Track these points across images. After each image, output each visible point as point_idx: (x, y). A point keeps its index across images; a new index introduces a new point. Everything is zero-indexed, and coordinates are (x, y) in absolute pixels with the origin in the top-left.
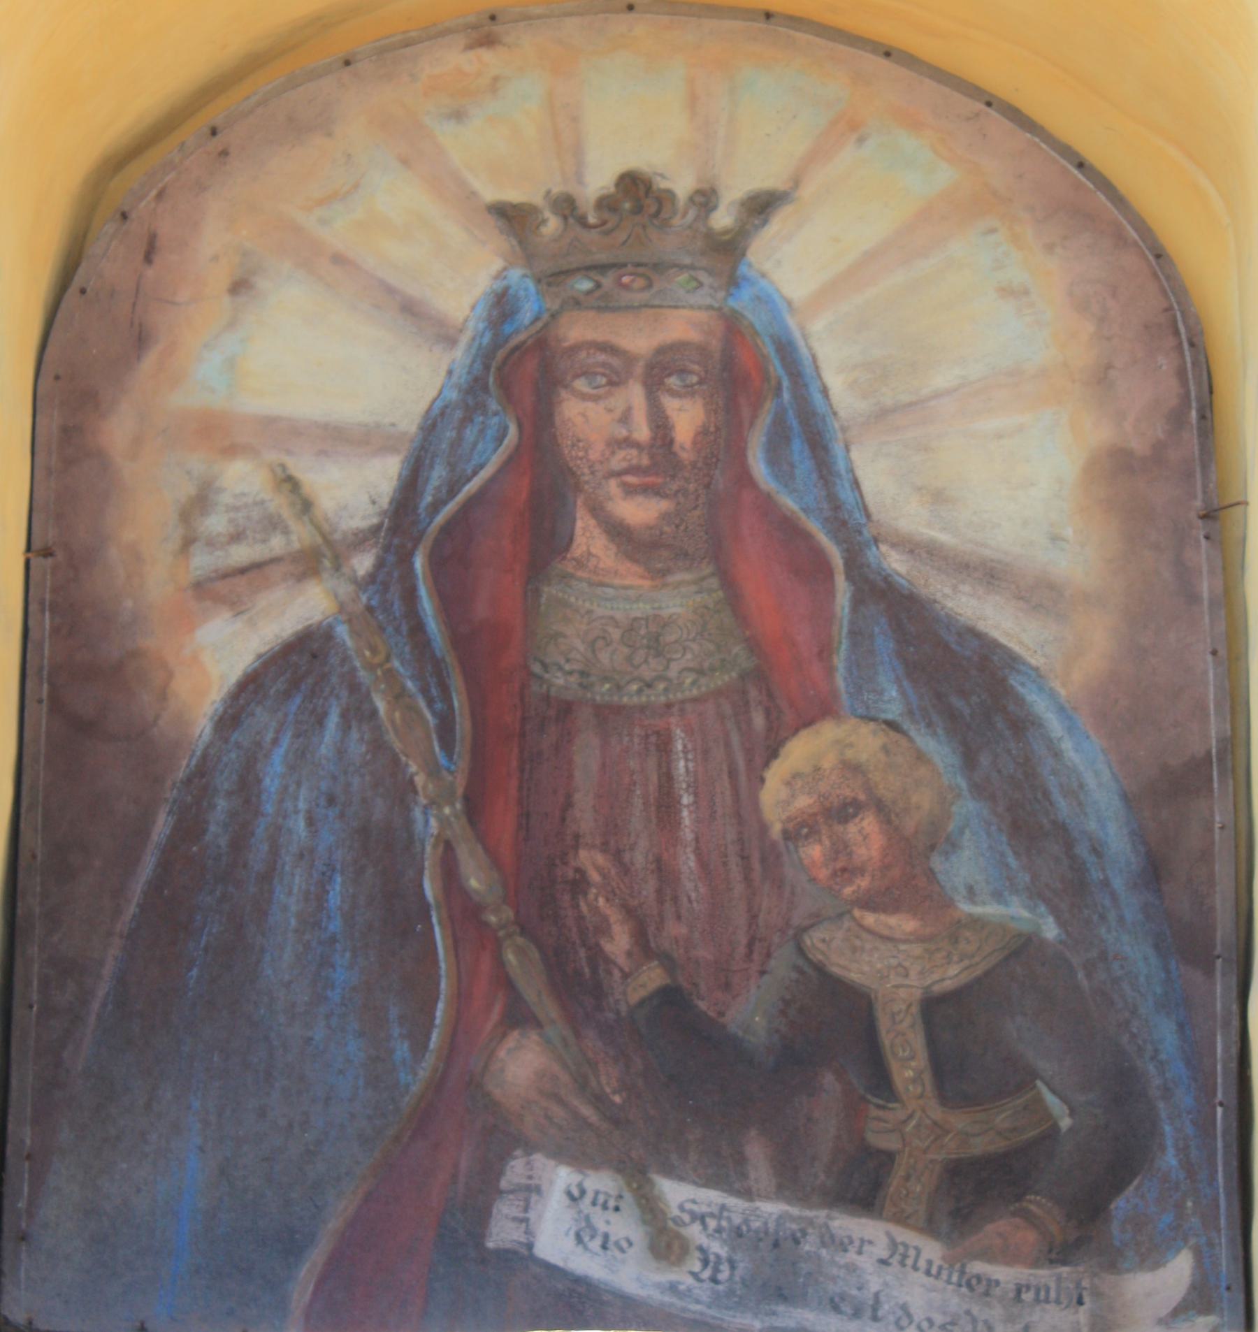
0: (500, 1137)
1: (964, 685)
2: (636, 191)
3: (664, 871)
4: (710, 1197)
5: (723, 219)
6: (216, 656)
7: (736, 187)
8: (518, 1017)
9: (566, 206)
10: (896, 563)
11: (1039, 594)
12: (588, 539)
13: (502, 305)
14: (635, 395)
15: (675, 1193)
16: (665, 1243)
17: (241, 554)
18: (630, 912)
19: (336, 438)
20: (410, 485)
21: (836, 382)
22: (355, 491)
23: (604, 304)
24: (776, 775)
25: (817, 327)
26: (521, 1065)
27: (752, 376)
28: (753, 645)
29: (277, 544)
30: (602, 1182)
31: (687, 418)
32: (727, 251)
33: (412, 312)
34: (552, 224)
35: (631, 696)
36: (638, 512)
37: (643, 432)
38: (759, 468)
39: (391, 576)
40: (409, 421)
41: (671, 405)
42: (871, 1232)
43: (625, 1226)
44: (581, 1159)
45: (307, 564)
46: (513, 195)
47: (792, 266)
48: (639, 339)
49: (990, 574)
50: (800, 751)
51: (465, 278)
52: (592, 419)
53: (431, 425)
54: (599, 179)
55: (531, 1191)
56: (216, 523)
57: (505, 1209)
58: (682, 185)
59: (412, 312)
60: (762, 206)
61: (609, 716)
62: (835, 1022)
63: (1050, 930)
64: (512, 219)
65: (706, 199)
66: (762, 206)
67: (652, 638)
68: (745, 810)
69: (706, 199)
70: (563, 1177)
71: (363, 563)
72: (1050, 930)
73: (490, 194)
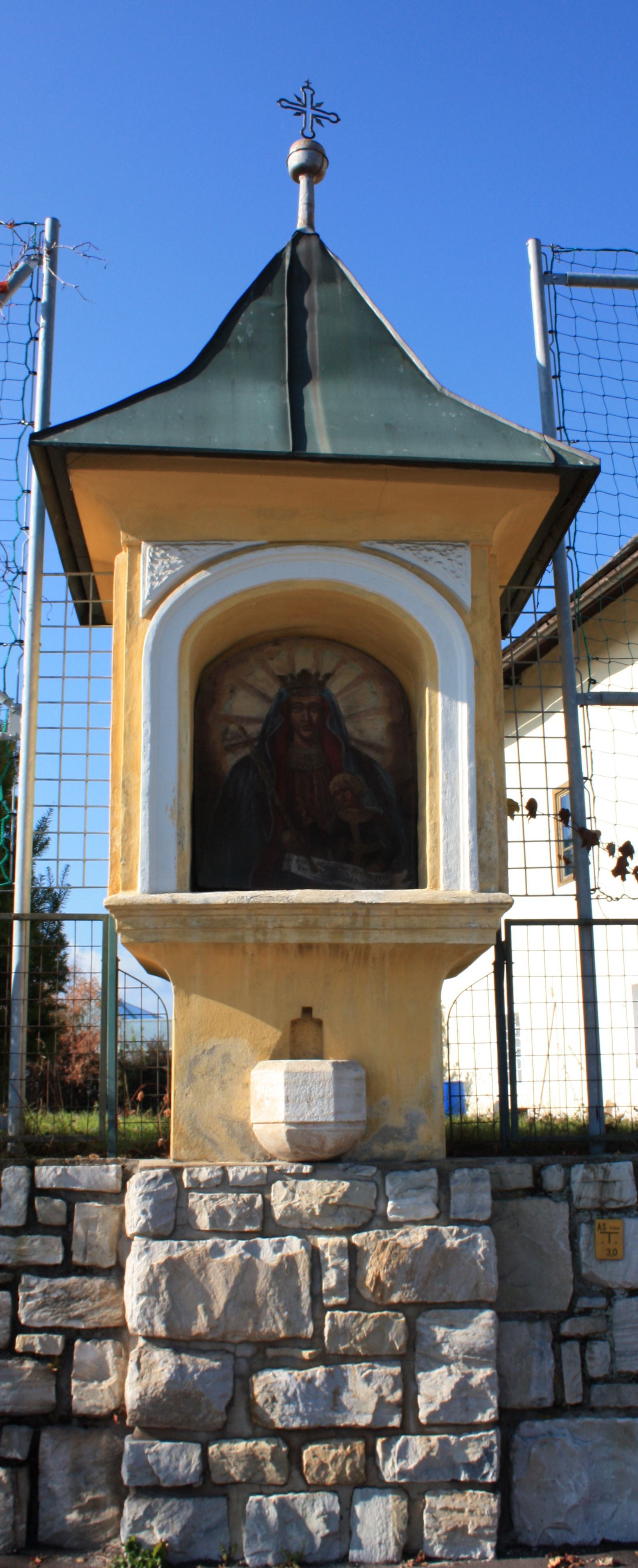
1: (365, 766)
2: (305, 673)
4: (321, 860)
5: (321, 679)
6: (231, 760)
7: (323, 672)
9: (292, 676)
10: (353, 744)
11: (378, 749)
12: (297, 739)
13: (280, 695)
14: (305, 712)
16: (314, 869)
17: (233, 742)
19: (251, 720)
21: (342, 710)
22: (254, 730)
25: (339, 699)
26: (287, 837)
27: (327, 708)
29: (240, 740)
30: (302, 858)
31: (315, 717)
32: (322, 686)
33: (263, 696)
34: (289, 680)
36: (306, 734)
37: (307, 719)
38: (328, 725)
40: (264, 716)
41: (312, 714)
42: (350, 867)
45: (246, 744)
46: (282, 674)
47: (334, 687)
48: (306, 701)
49: (370, 745)
50: (336, 779)
51: (273, 690)
52: (297, 716)
54: (298, 670)
56: (229, 736)
58: (313, 672)
60: (328, 676)
63: (382, 812)
64: (282, 679)
65: (318, 674)
66: (328, 676)
69: (318, 674)
71: (256, 744)
72: (382, 812)
73: (278, 673)
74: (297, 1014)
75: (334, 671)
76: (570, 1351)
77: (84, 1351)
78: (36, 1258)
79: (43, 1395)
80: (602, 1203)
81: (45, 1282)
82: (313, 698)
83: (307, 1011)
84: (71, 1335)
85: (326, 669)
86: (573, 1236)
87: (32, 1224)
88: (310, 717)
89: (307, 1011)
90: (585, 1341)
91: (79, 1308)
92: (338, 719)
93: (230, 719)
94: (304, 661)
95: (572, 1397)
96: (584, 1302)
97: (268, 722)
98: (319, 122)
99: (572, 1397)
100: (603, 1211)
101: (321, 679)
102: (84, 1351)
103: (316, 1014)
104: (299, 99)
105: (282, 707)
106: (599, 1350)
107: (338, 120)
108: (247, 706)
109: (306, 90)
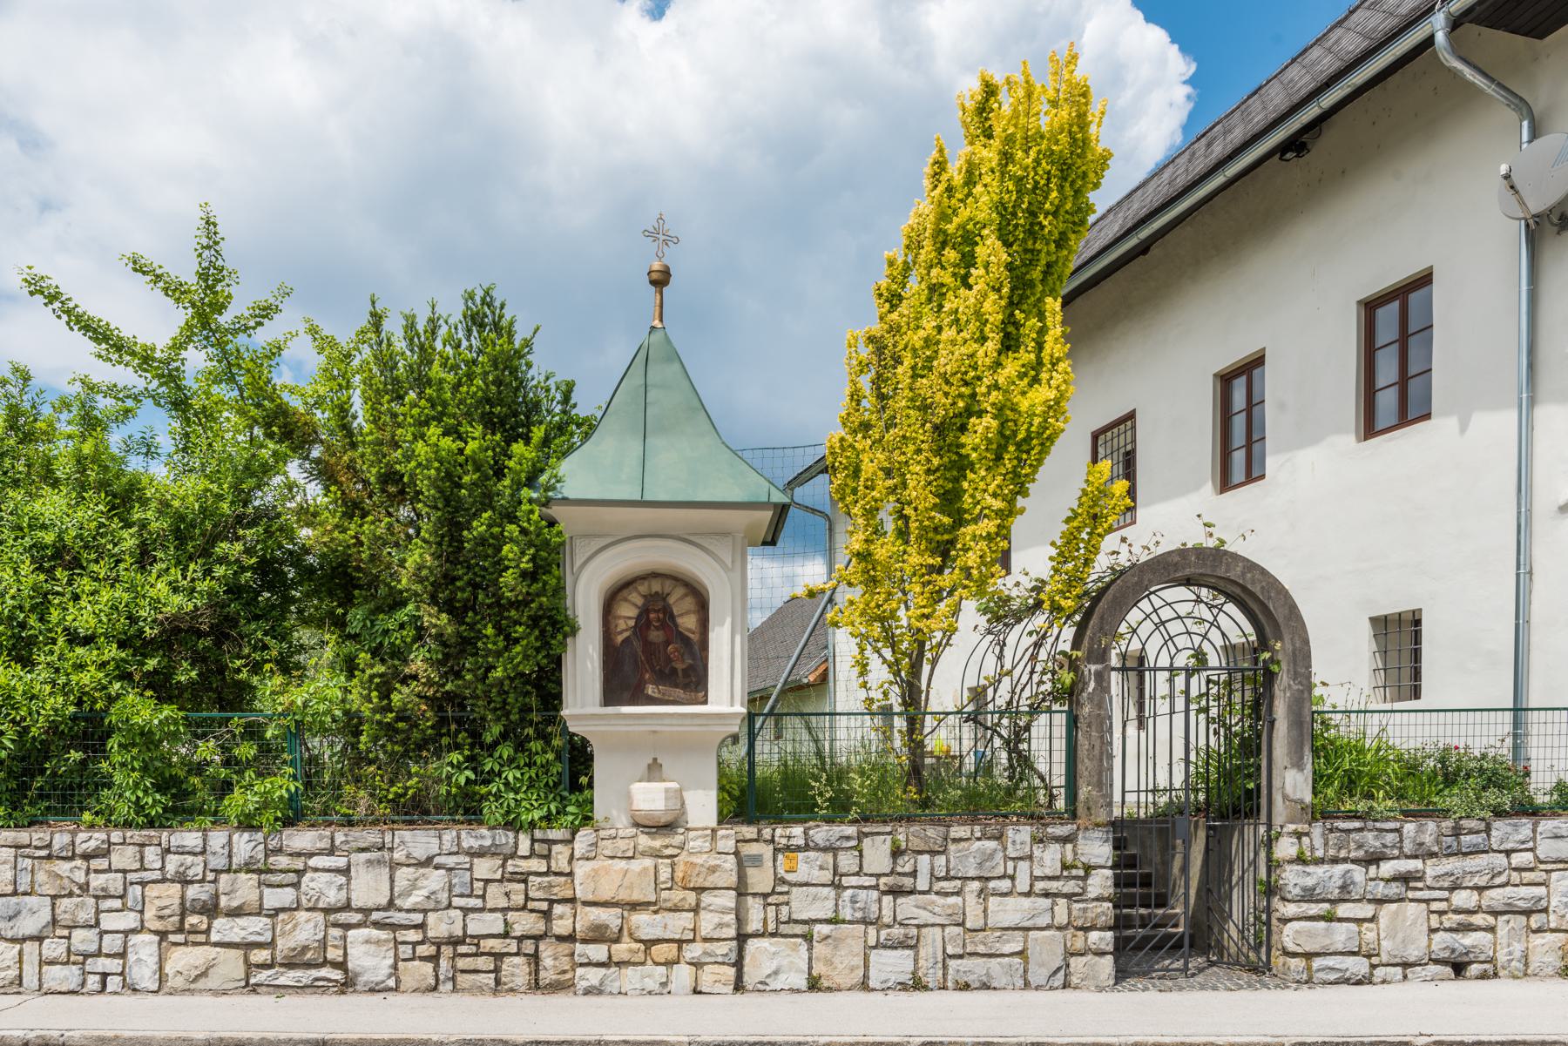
1: (686, 641)
6: (620, 639)
22: (632, 623)
32: (664, 599)
33: (635, 605)
39: (634, 633)
47: (671, 600)
62: (674, 671)
76: (771, 910)
77: (558, 909)
78: (534, 869)
79: (540, 927)
81: (539, 879)
82: (660, 605)
84: (551, 902)
85: (667, 590)
86: (775, 860)
87: (533, 854)
90: (777, 905)
91: (555, 890)
92: (672, 617)
94: (656, 586)
95: (771, 927)
96: (779, 889)
97: (638, 619)
99: (771, 927)
100: (788, 848)
102: (558, 909)
105: (644, 612)
106: (784, 910)
108: (627, 612)
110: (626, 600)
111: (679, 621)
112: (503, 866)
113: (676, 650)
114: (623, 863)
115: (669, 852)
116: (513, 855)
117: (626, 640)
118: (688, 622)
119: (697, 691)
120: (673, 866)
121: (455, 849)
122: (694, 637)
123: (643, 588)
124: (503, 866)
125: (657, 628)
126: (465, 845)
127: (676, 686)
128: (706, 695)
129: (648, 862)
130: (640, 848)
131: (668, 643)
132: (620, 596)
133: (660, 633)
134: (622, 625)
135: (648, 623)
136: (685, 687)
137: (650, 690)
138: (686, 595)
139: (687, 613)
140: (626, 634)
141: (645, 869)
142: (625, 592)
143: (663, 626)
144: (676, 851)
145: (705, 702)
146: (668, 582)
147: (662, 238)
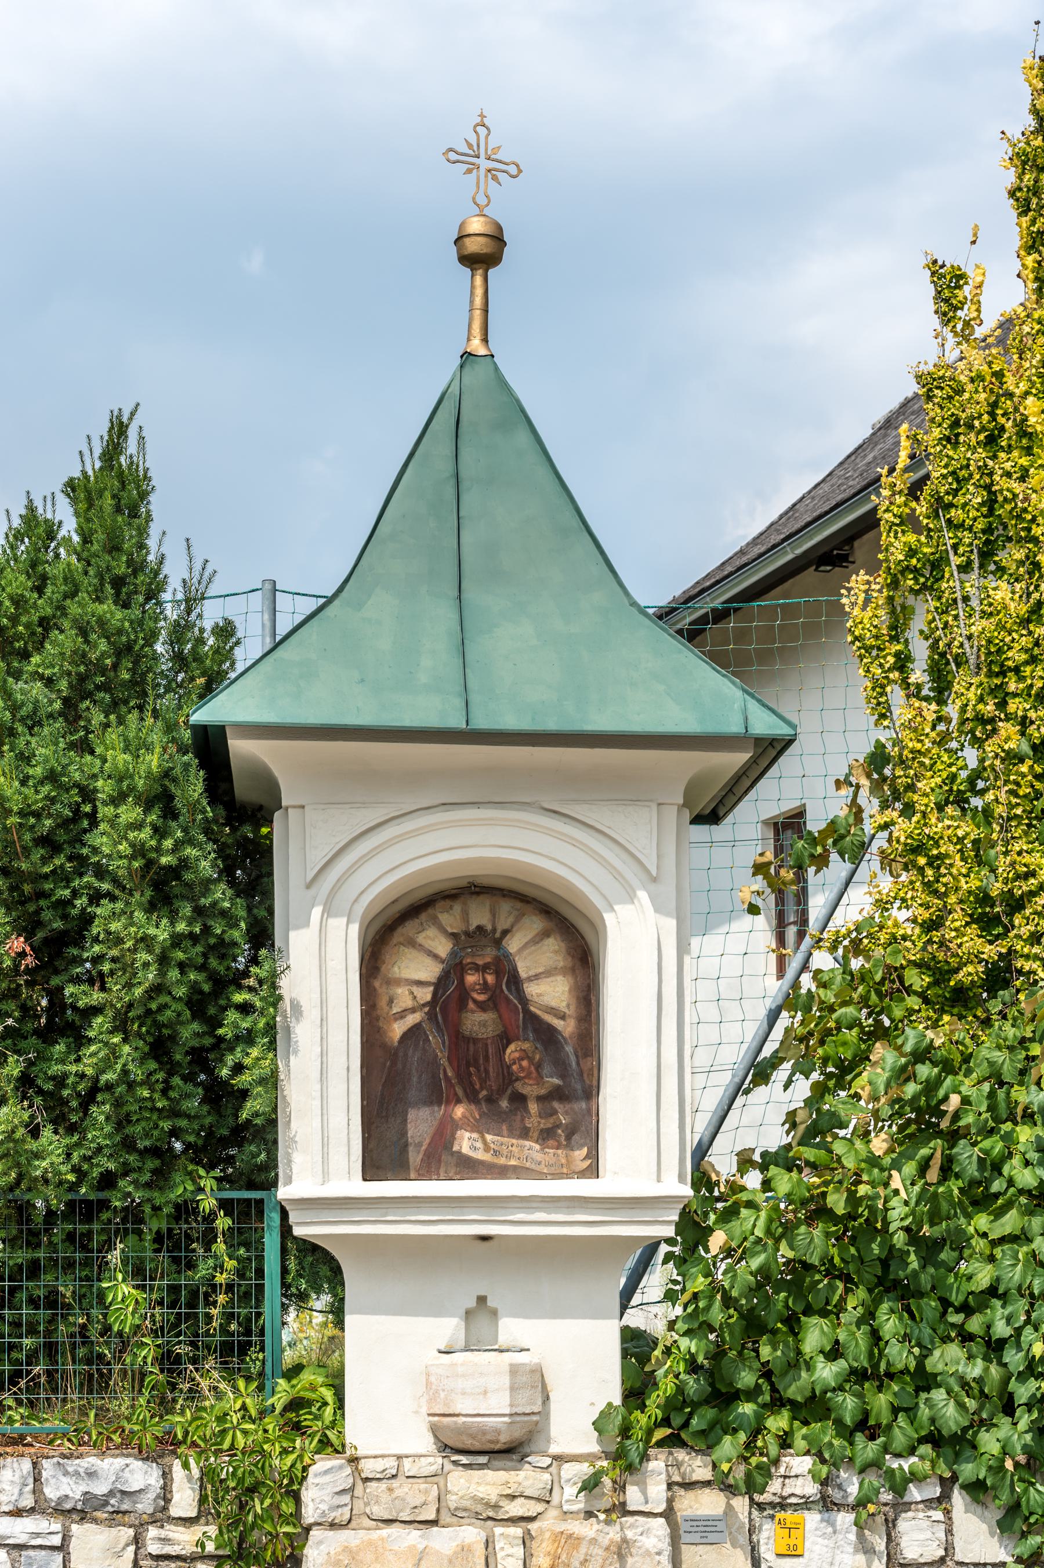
0: (456, 1126)
1: (547, 1036)
2: (480, 928)
3: (487, 1071)
4: (496, 1138)
5: (498, 935)
6: (397, 1030)
8: (459, 1101)
12: (471, 1005)
13: (453, 954)
15: (489, 1137)
16: (487, 1148)
18: (480, 1078)
19: (420, 983)
20: (435, 994)
22: (425, 995)
23: (473, 955)
24: (508, 1051)
26: (459, 1111)
28: (504, 1026)
30: (475, 1135)
32: (498, 943)
33: (435, 956)
35: (480, 1036)
36: (481, 998)
39: (431, 1016)
40: (434, 980)
42: (527, 1143)
43: (479, 1144)
44: (472, 1131)
45: (413, 1010)
47: (513, 945)
50: (512, 1047)
51: (443, 947)
53: (440, 979)
54: (472, 928)
55: (462, 1138)
57: (456, 1143)
58: (489, 927)
59: (435, 956)
60: (505, 932)
61: (475, 1041)
64: (454, 935)
65: (494, 930)
67: (483, 1024)
68: (501, 1059)
70: (467, 1135)
71: (426, 1009)
73: (450, 930)
74: (472, 1303)
75: (512, 926)
80: (784, 1498)
82: (487, 956)
83: (482, 1300)
85: (503, 924)
88: (484, 979)
89: (482, 1300)
92: (515, 981)
93: (398, 982)
94: (479, 916)
97: (440, 985)
98: (495, 178)
101: (498, 935)
103: (490, 1303)
104: (470, 146)
105: (453, 971)
107: (520, 171)
108: (416, 969)
109: (479, 129)
110: (412, 943)
111: (532, 990)
112: (137, 1541)
113: (525, 1055)
114: (413, 1537)
115: (516, 1509)
116: (161, 1515)
117: (414, 1031)
118: (551, 993)
119: (569, 1146)
120: (526, 1540)
121: (28, 1502)
122: (567, 1028)
123: (451, 919)
124: (137, 1541)
125: (482, 1006)
126: (51, 1492)
127: (525, 1134)
128: (594, 1155)
129: (472, 1534)
130: (452, 1501)
131: (505, 1039)
132: (398, 936)
133: (489, 1016)
134: (403, 998)
135: (463, 995)
136: (546, 1136)
137: (466, 1143)
138: (545, 934)
139: (548, 973)
140: (412, 1019)
141: (465, 1549)
142: (409, 928)
143: (493, 1002)
144: (531, 1508)
145: (593, 1171)
146: (505, 907)
147: (484, 164)
